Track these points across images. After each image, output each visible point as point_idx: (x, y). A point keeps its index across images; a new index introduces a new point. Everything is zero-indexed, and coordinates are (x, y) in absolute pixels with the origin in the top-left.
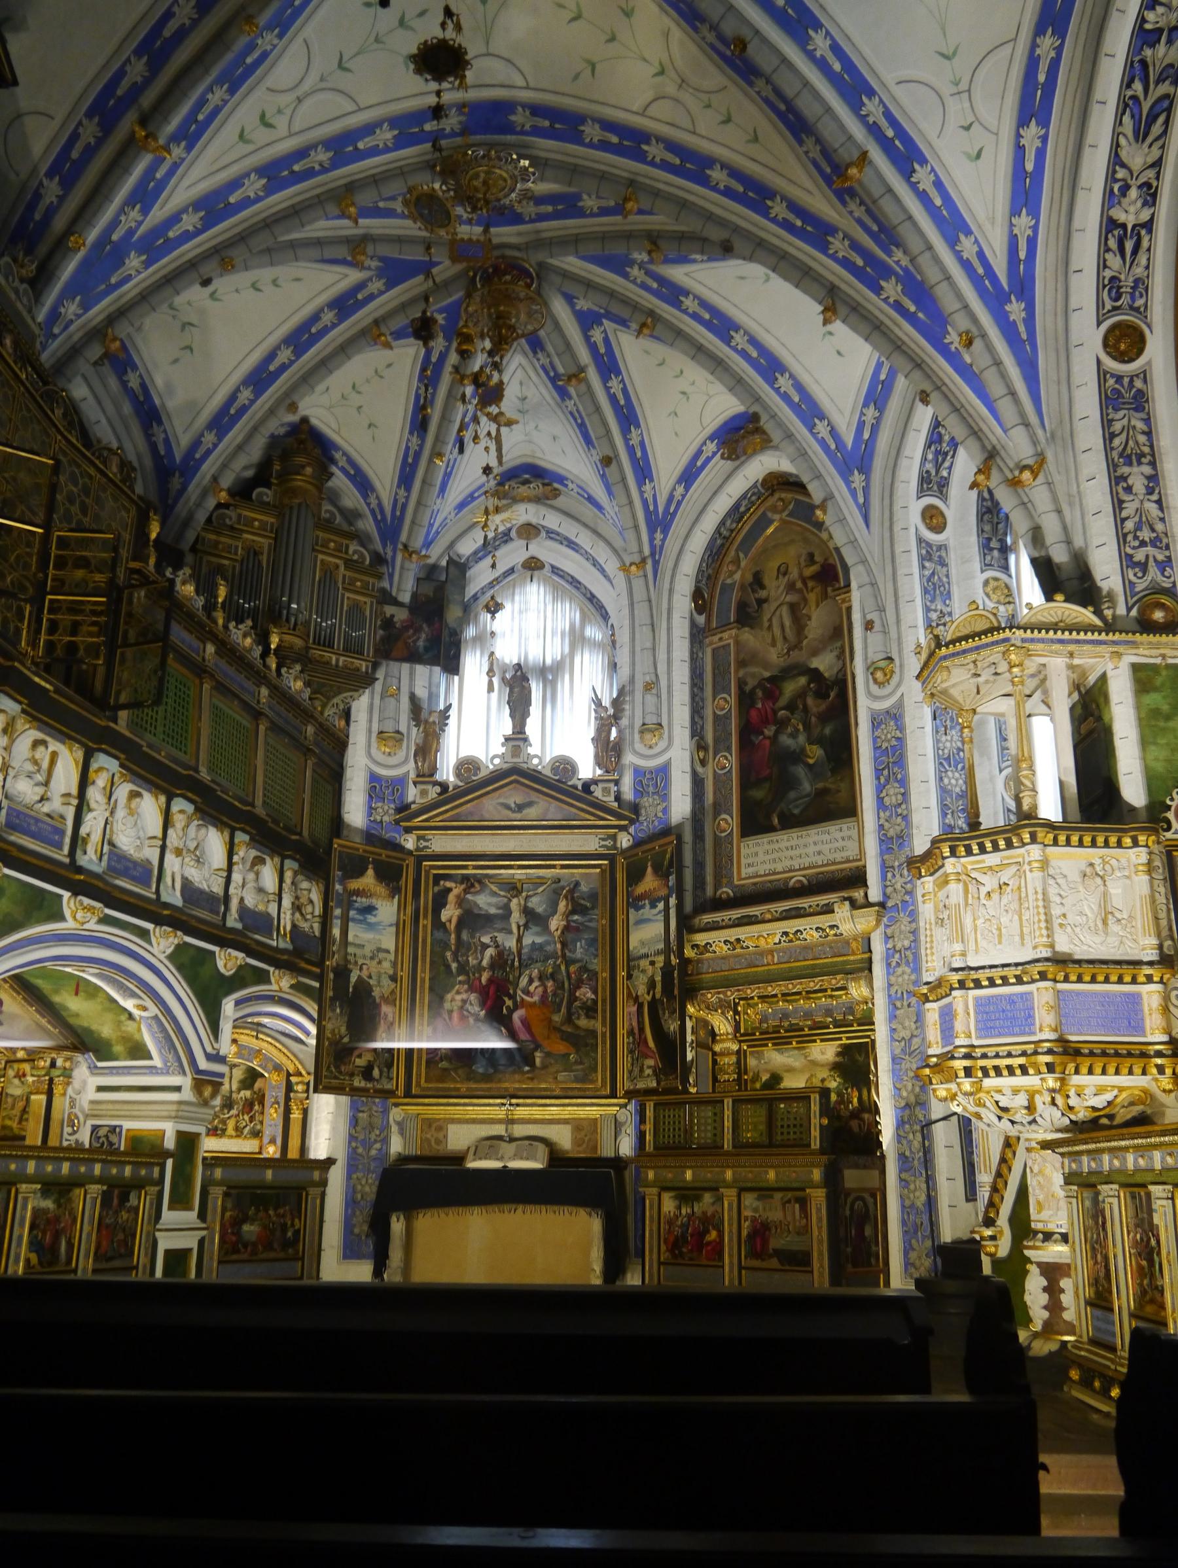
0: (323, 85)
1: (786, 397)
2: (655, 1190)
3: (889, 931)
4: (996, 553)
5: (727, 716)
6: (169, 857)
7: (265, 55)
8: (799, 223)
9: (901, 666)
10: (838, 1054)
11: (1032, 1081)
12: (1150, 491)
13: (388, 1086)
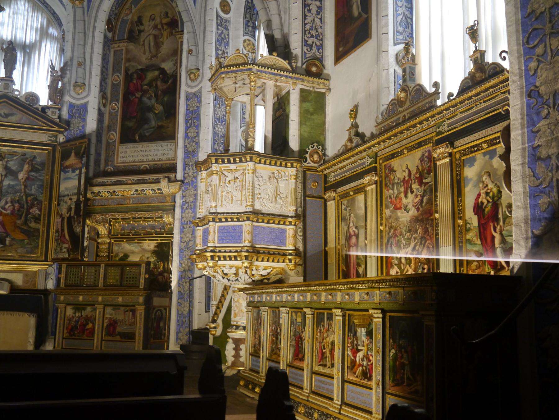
2: (63, 305)
3: (184, 194)
4: (250, 28)
5: (118, 85)
9: (203, 73)
10: (156, 247)
11: (238, 263)
12: (318, 14)
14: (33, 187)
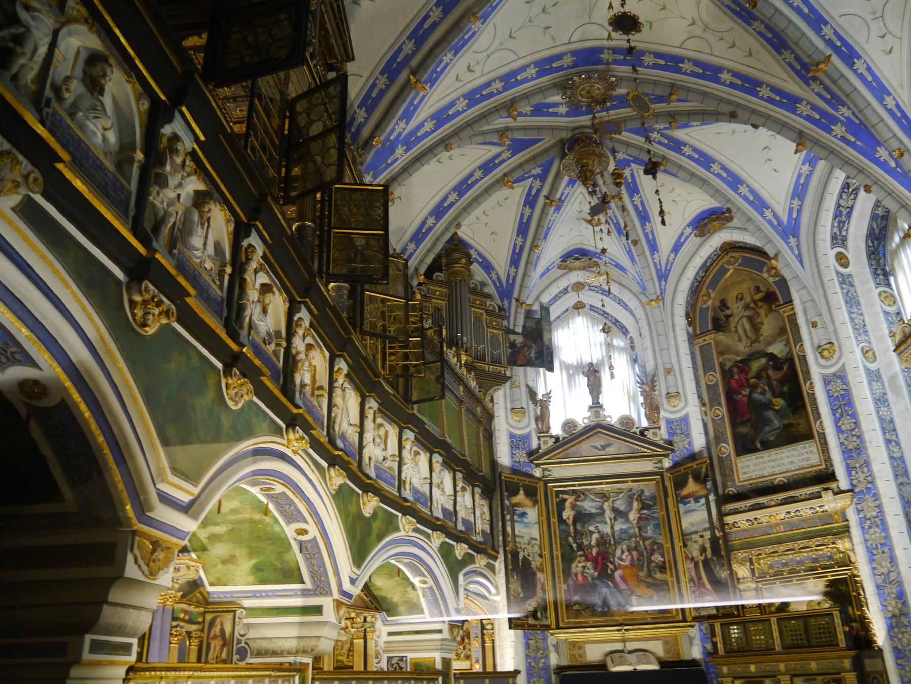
0: (501, 47)
1: (745, 198)
2: (730, 679)
3: (859, 507)
4: (881, 277)
5: (716, 385)
6: (435, 489)
7: (474, 33)
8: (778, 98)
9: (840, 347)
10: (827, 586)
13: (546, 623)
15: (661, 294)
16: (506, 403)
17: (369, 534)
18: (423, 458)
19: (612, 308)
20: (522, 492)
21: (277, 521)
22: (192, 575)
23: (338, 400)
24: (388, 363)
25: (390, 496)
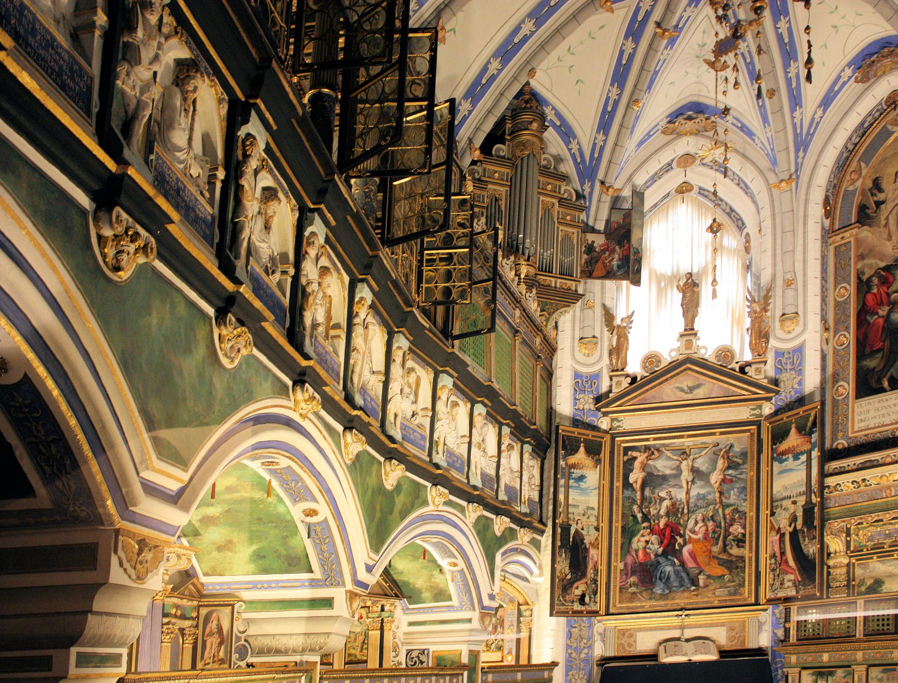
14: (732, 492)
15: (796, 171)
16: (574, 330)
17: (391, 511)
18: (463, 409)
19: (728, 192)
20: (582, 449)
21: (280, 500)
22: (183, 565)
23: (358, 341)
24: (424, 285)
25: (418, 462)
